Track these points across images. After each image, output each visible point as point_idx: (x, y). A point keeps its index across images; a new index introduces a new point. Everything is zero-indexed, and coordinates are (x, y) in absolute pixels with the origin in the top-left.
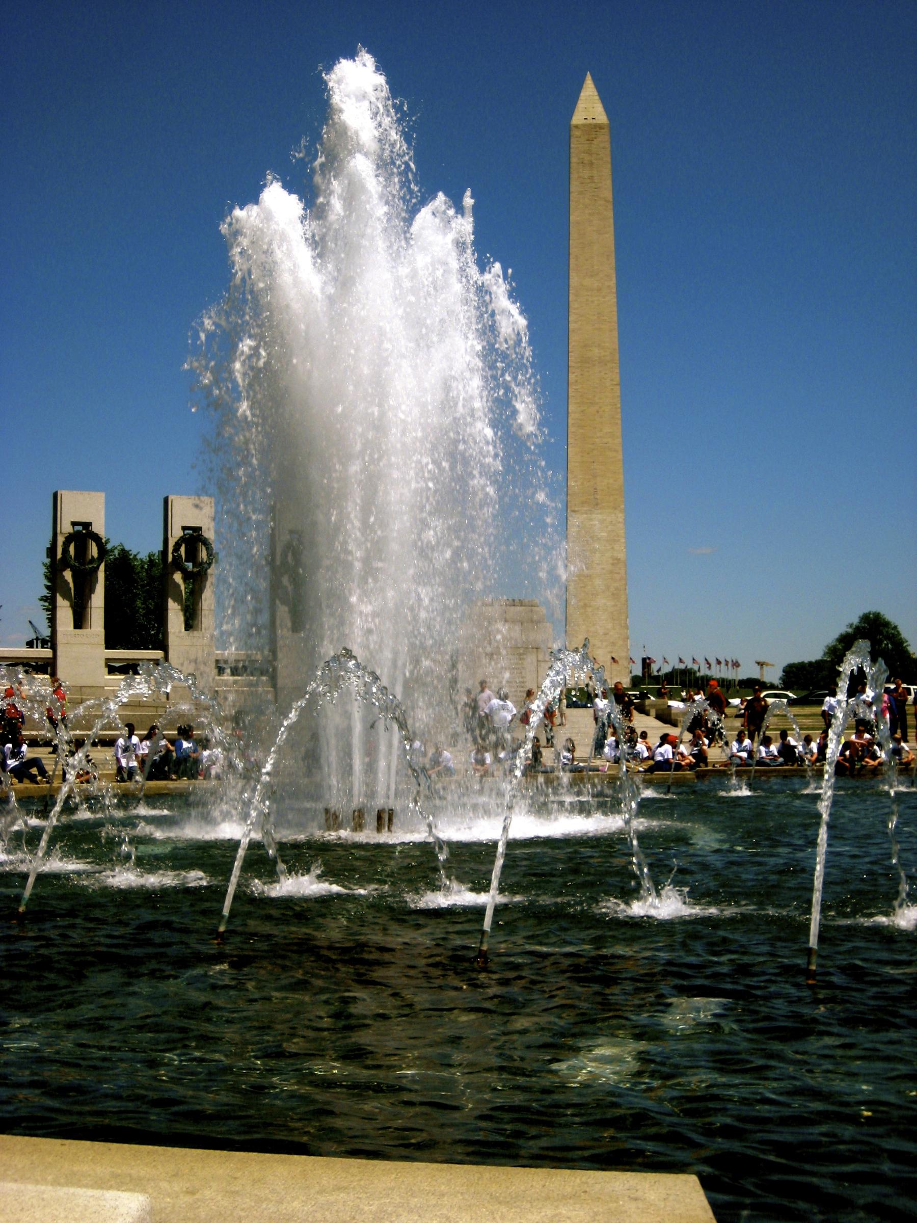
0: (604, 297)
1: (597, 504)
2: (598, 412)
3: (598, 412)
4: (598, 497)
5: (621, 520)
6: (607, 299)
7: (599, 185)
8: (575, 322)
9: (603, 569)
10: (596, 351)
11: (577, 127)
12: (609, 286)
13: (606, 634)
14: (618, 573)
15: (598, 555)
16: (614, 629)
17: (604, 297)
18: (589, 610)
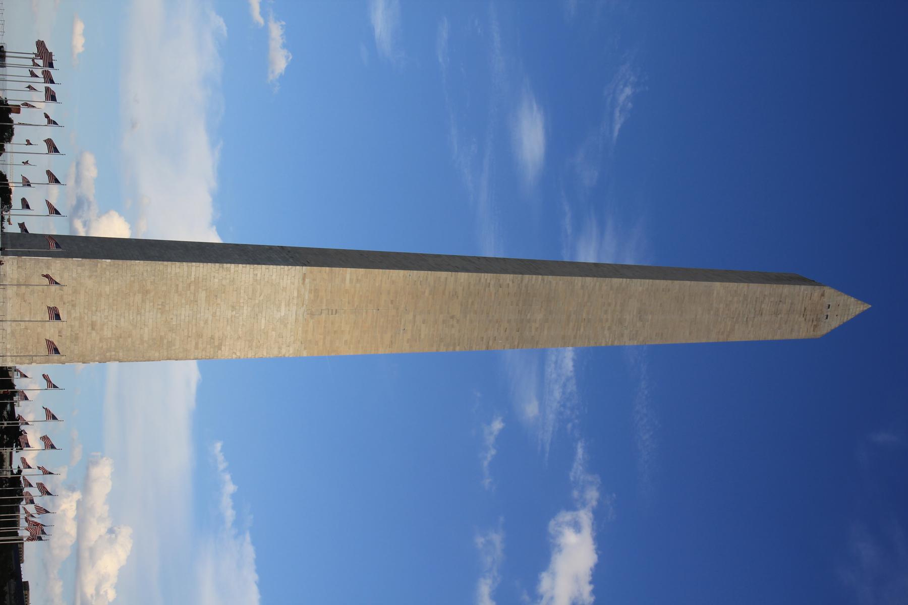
0: (609, 328)
1: (312, 315)
2: (452, 317)
3: (452, 317)
4: (324, 316)
5: (283, 351)
6: (606, 332)
7: (750, 323)
8: (582, 287)
9: (206, 322)
10: (539, 316)
11: (823, 295)
12: (622, 335)
13: (93, 326)
14: (196, 347)
15: (229, 314)
16: (101, 340)
17: (609, 328)
18: (138, 297)
